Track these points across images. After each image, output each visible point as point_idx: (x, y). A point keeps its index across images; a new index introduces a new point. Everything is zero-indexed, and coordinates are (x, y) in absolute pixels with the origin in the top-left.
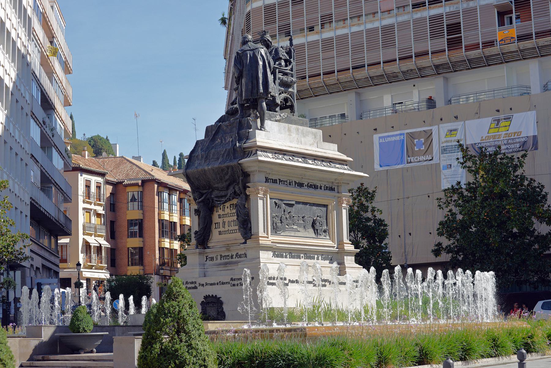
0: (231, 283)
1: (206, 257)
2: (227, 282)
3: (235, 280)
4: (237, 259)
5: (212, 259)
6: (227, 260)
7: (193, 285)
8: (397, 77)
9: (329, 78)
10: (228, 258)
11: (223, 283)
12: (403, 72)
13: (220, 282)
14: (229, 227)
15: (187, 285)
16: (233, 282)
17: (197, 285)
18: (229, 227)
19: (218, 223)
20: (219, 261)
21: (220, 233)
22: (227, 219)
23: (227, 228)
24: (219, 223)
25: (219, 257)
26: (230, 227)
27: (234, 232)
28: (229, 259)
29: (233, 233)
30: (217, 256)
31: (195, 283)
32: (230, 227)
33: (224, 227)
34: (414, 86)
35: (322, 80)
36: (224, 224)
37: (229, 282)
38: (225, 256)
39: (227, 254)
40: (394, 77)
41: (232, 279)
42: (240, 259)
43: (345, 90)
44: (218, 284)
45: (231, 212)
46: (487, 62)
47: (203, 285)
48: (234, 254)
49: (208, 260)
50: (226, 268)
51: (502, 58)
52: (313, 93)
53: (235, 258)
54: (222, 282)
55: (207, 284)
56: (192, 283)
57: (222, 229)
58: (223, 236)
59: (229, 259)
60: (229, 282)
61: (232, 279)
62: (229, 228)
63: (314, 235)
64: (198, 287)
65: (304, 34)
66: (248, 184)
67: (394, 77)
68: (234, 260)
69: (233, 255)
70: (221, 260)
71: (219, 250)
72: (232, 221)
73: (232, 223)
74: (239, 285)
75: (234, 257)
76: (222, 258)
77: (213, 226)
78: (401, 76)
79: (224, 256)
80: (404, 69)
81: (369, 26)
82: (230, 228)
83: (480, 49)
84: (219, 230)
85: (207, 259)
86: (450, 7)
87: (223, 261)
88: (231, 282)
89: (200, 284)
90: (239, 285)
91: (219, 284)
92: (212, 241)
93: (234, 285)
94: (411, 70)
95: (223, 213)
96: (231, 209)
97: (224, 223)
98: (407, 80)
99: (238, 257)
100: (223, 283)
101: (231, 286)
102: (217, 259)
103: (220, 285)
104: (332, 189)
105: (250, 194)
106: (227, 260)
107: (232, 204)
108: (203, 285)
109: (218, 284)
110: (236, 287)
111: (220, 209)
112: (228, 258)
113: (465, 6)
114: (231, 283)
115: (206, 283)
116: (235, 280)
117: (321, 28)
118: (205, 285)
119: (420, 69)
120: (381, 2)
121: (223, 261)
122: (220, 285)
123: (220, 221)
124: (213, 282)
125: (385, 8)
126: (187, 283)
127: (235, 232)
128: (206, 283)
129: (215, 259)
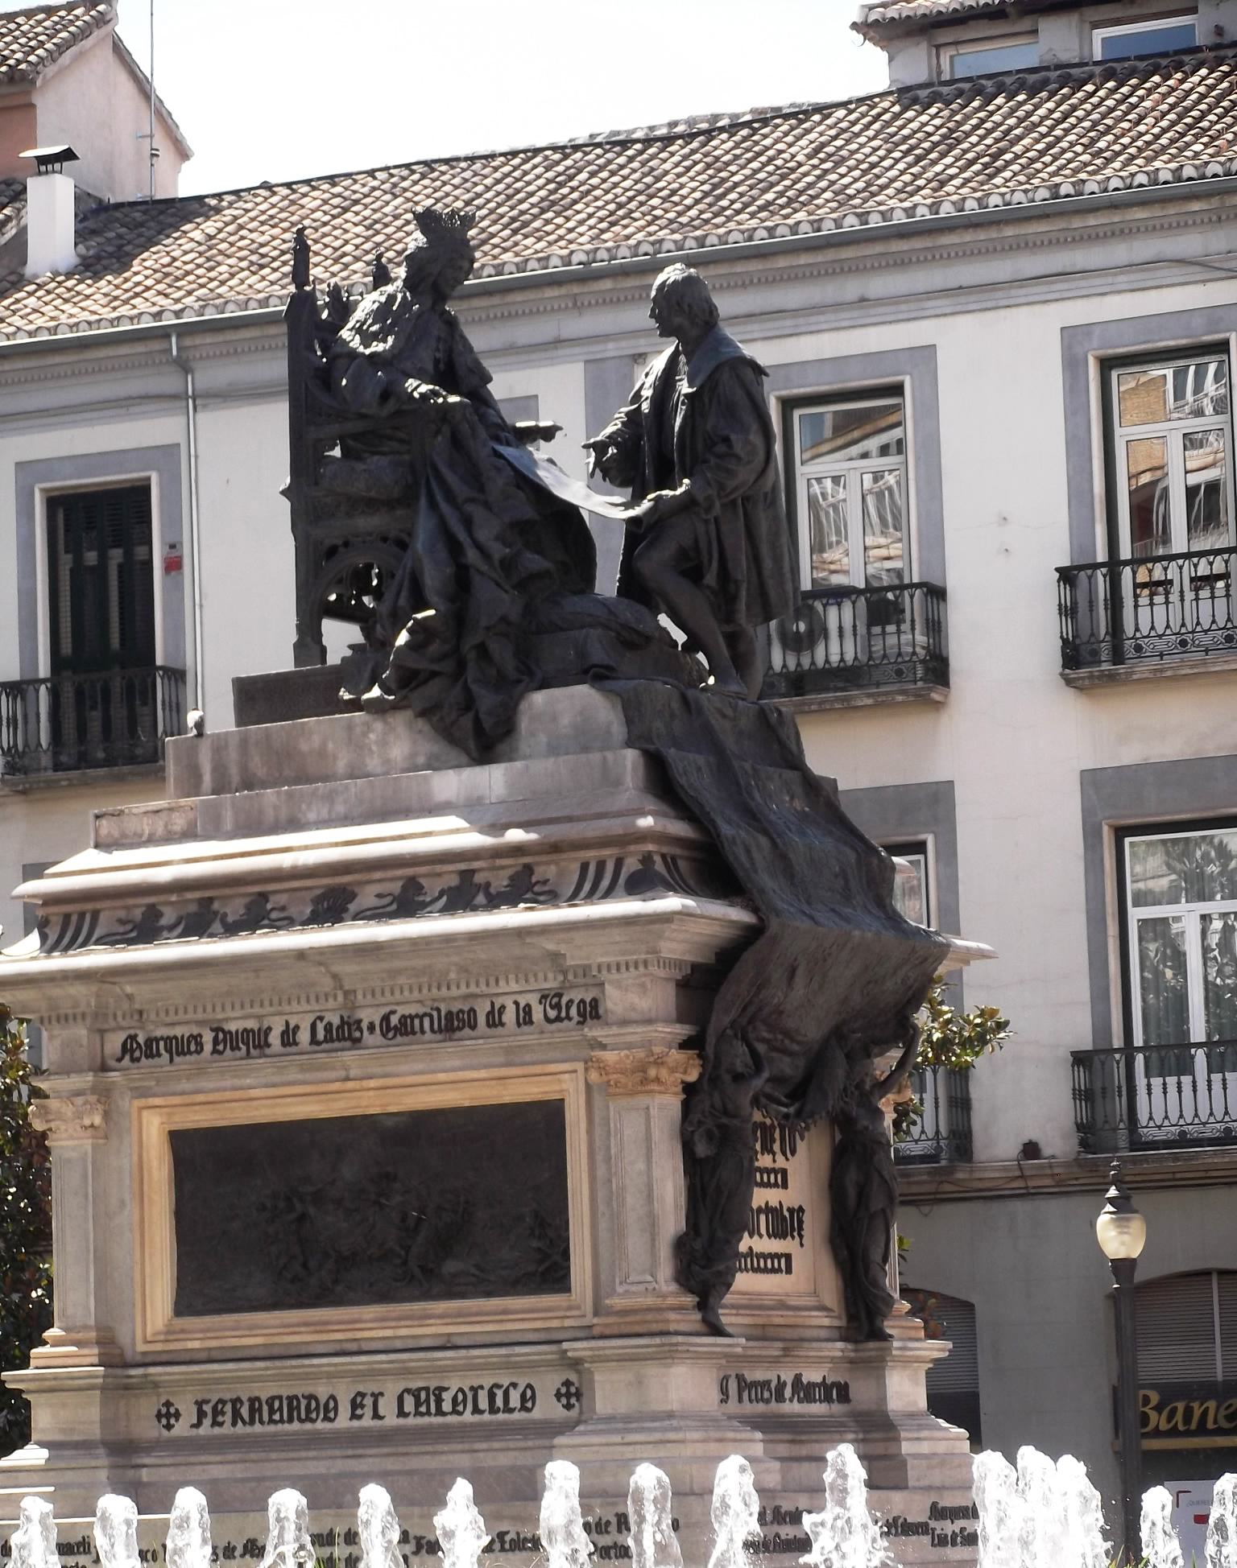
10: (766, 1395)
13: (895, 1519)
26: (756, 1237)
32: (756, 1237)
37: (926, 1524)
48: (788, 1377)
54: (901, 1521)
60: (926, 1524)
61: (938, 1512)
71: (756, 1352)
76: (745, 1395)
87: (749, 1408)
88: (932, 1524)
93: (941, 1541)
101: (933, 1545)
106: (761, 1407)
112: (766, 1395)
114: (933, 1530)
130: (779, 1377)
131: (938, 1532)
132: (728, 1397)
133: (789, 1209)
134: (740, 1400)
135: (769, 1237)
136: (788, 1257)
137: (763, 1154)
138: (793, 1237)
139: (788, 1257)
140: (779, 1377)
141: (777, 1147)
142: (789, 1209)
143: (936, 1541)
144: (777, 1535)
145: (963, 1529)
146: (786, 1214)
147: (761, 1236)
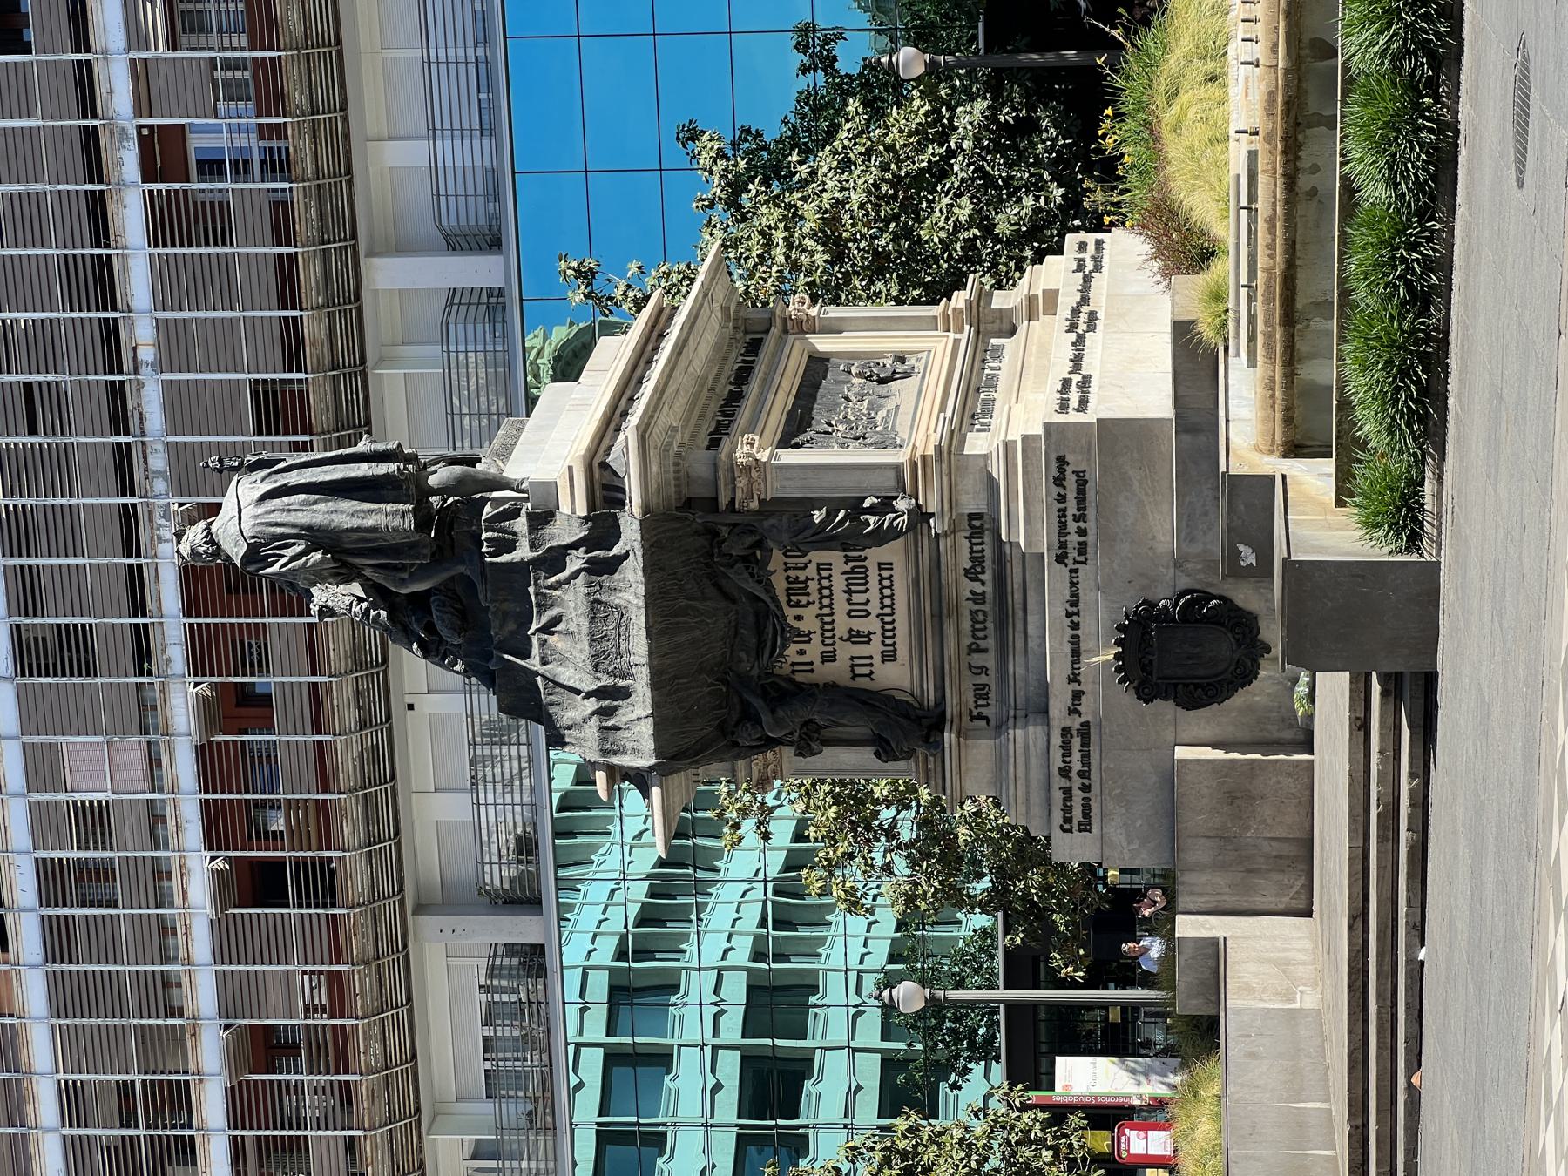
0: (1076, 562)
1: (972, 718)
2: (1071, 583)
3: (1063, 545)
4: (986, 577)
5: (981, 692)
6: (990, 625)
7: (1076, 743)
8: (374, 748)
9: (356, 995)
10: (981, 617)
11: (1075, 600)
12: (363, 725)
13: (1069, 615)
14: (869, 614)
15: (1073, 774)
16: (1073, 553)
17: (1076, 723)
18: (869, 614)
19: (853, 666)
20: (990, 660)
21: (889, 656)
22: (842, 624)
23: (872, 624)
24: (852, 658)
25: (977, 660)
27: (887, 592)
28: (985, 613)
29: (891, 597)
30: (970, 667)
31: (1066, 731)
33: (866, 638)
34: (411, 707)
35: (360, 1022)
36: (859, 634)
38: (974, 630)
39: (967, 624)
40: (375, 761)
41: (1061, 559)
42: (988, 563)
43: (405, 946)
44: (1075, 626)
45: (817, 605)
46: (354, 426)
47: (1077, 696)
48: (967, 586)
49: (985, 711)
50: (1020, 614)
51: (347, 370)
52: (402, 1064)
53: (983, 583)
54: (1068, 606)
55: (1074, 678)
56: (1066, 747)
57: (875, 648)
58: (902, 651)
59: (985, 613)
60: (1071, 571)
61: (1061, 559)
62: (873, 615)
63: (913, 382)
64: (1083, 719)
65: (192, 1085)
66: (724, 501)
67: (375, 761)
68: (988, 589)
69: (971, 592)
70: (985, 651)
72: (849, 600)
73: (856, 598)
74: (1082, 524)
75: (978, 588)
76: (982, 644)
77: (863, 683)
78: (373, 737)
79: (974, 636)
80: (351, 717)
81: (193, 833)
82: (875, 607)
83: (311, 441)
84: (877, 659)
85: (980, 717)
86: (160, 540)
88: (1069, 561)
89: (1074, 711)
90: (1082, 524)
91: (1075, 619)
92: (917, 692)
93: (1082, 549)
94: (358, 693)
95: (816, 638)
96: (804, 600)
97: (855, 636)
98: (389, 718)
99: (979, 570)
100: (1075, 600)
101: (1085, 563)
102: (984, 670)
103: (1078, 614)
104: (754, 347)
105: (756, 497)
107: (789, 595)
108: (1077, 696)
109: (1075, 626)
110: (1090, 539)
111: (802, 652)
113: (160, 486)
114: (1076, 562)
115: (1070, 681)
116: (1063, 545)
117: (181, 1015)
118: (1075, 686)
119: (358, 665)
120: (115, 789)
121: (990, 643)
122: (1078, 614)
123: (845, 651)
124: (1068, 648)
125: (138, 773)
126: (1065, 772)
127: (890, 587)
128: (1070, 681)
129: (983, 679)
130: (968, 599)
131: (1075, 553)
132: (982, 668)
133: (846, 563)
134: (985, 651)
135: (867, 590)
136: (881, 566)
137: (808, 594)
138: (866, 558)
139: (881, 566)
140: (968, 599)
141: (802, 575)
142: (846, 563)
143: (1082, 558)
144: (1078, 773)
145: (1076, 519)
146: (848, 568)
147: (868, 601)
